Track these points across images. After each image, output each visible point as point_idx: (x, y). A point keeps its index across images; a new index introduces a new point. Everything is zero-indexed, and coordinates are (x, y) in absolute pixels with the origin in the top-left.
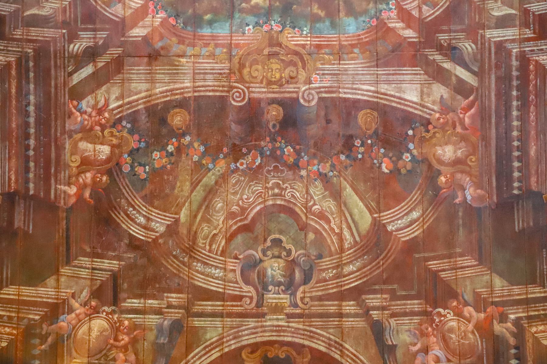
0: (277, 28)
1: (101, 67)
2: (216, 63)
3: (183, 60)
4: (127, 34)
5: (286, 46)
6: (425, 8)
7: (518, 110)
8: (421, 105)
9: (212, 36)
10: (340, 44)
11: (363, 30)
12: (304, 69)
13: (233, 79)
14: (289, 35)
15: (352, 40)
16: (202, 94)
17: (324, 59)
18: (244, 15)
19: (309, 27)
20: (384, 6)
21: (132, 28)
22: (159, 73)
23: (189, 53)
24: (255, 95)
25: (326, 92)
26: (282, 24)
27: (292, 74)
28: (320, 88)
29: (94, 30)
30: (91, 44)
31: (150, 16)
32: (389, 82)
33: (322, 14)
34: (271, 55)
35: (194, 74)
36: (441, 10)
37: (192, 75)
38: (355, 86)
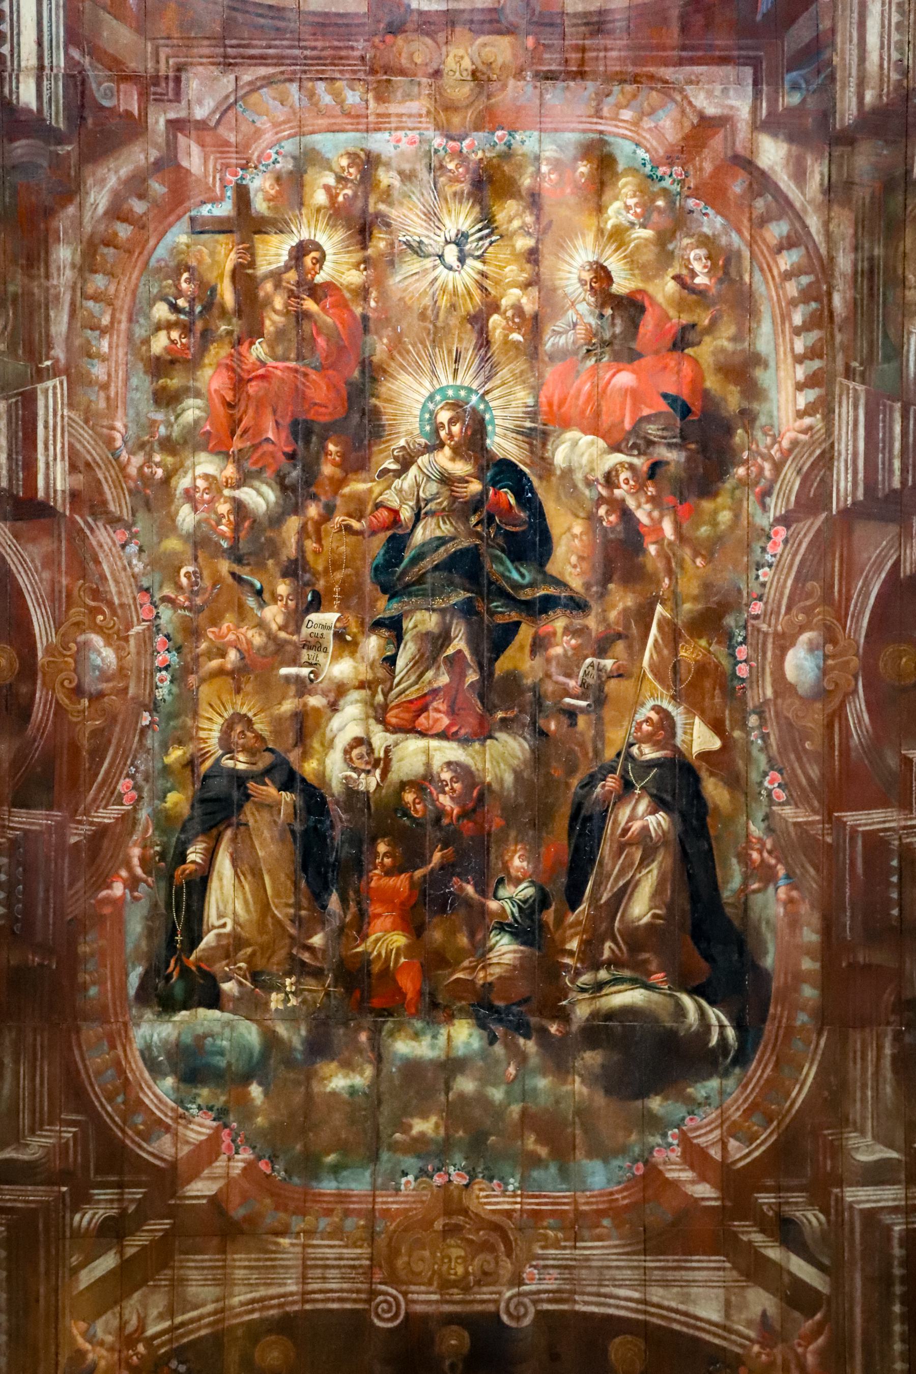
0: (459, 1180)
1: (134, 1256)
2: (346, 1247)
3: (285, 1241)
4: (179, 1193)
5: (476, 1215)
6: (733, 1143)
7: (903, 1341)
8: (724, 1328)
9: (339, 1195)
10: (576, 1210)
11: (619, 1183)
12: (509, 1256)
13: (378, 1276)
14: (482, 1194)
15: (597, 1203)
16: (320, 1306)
17: (546, 1237)
18: (399, 1156)
19: (518, 1177)
20: (658, 1140)
21: (189, 1182)
22: (240, 1267)
23: (295, 1229)
24: (419, 1308)
25: (549, 1301)
26: (468, 1173)
27: (487, 1268)
28: (539, 1292)
29: (120, 1185)
31: (224, 1157)
32: (666, 1284)
33: (543, 1151)
34: (451, 1231)
35: (305, 1267)
36: (763, 1148)
37: (300, 1269)
38: (603, 1290)
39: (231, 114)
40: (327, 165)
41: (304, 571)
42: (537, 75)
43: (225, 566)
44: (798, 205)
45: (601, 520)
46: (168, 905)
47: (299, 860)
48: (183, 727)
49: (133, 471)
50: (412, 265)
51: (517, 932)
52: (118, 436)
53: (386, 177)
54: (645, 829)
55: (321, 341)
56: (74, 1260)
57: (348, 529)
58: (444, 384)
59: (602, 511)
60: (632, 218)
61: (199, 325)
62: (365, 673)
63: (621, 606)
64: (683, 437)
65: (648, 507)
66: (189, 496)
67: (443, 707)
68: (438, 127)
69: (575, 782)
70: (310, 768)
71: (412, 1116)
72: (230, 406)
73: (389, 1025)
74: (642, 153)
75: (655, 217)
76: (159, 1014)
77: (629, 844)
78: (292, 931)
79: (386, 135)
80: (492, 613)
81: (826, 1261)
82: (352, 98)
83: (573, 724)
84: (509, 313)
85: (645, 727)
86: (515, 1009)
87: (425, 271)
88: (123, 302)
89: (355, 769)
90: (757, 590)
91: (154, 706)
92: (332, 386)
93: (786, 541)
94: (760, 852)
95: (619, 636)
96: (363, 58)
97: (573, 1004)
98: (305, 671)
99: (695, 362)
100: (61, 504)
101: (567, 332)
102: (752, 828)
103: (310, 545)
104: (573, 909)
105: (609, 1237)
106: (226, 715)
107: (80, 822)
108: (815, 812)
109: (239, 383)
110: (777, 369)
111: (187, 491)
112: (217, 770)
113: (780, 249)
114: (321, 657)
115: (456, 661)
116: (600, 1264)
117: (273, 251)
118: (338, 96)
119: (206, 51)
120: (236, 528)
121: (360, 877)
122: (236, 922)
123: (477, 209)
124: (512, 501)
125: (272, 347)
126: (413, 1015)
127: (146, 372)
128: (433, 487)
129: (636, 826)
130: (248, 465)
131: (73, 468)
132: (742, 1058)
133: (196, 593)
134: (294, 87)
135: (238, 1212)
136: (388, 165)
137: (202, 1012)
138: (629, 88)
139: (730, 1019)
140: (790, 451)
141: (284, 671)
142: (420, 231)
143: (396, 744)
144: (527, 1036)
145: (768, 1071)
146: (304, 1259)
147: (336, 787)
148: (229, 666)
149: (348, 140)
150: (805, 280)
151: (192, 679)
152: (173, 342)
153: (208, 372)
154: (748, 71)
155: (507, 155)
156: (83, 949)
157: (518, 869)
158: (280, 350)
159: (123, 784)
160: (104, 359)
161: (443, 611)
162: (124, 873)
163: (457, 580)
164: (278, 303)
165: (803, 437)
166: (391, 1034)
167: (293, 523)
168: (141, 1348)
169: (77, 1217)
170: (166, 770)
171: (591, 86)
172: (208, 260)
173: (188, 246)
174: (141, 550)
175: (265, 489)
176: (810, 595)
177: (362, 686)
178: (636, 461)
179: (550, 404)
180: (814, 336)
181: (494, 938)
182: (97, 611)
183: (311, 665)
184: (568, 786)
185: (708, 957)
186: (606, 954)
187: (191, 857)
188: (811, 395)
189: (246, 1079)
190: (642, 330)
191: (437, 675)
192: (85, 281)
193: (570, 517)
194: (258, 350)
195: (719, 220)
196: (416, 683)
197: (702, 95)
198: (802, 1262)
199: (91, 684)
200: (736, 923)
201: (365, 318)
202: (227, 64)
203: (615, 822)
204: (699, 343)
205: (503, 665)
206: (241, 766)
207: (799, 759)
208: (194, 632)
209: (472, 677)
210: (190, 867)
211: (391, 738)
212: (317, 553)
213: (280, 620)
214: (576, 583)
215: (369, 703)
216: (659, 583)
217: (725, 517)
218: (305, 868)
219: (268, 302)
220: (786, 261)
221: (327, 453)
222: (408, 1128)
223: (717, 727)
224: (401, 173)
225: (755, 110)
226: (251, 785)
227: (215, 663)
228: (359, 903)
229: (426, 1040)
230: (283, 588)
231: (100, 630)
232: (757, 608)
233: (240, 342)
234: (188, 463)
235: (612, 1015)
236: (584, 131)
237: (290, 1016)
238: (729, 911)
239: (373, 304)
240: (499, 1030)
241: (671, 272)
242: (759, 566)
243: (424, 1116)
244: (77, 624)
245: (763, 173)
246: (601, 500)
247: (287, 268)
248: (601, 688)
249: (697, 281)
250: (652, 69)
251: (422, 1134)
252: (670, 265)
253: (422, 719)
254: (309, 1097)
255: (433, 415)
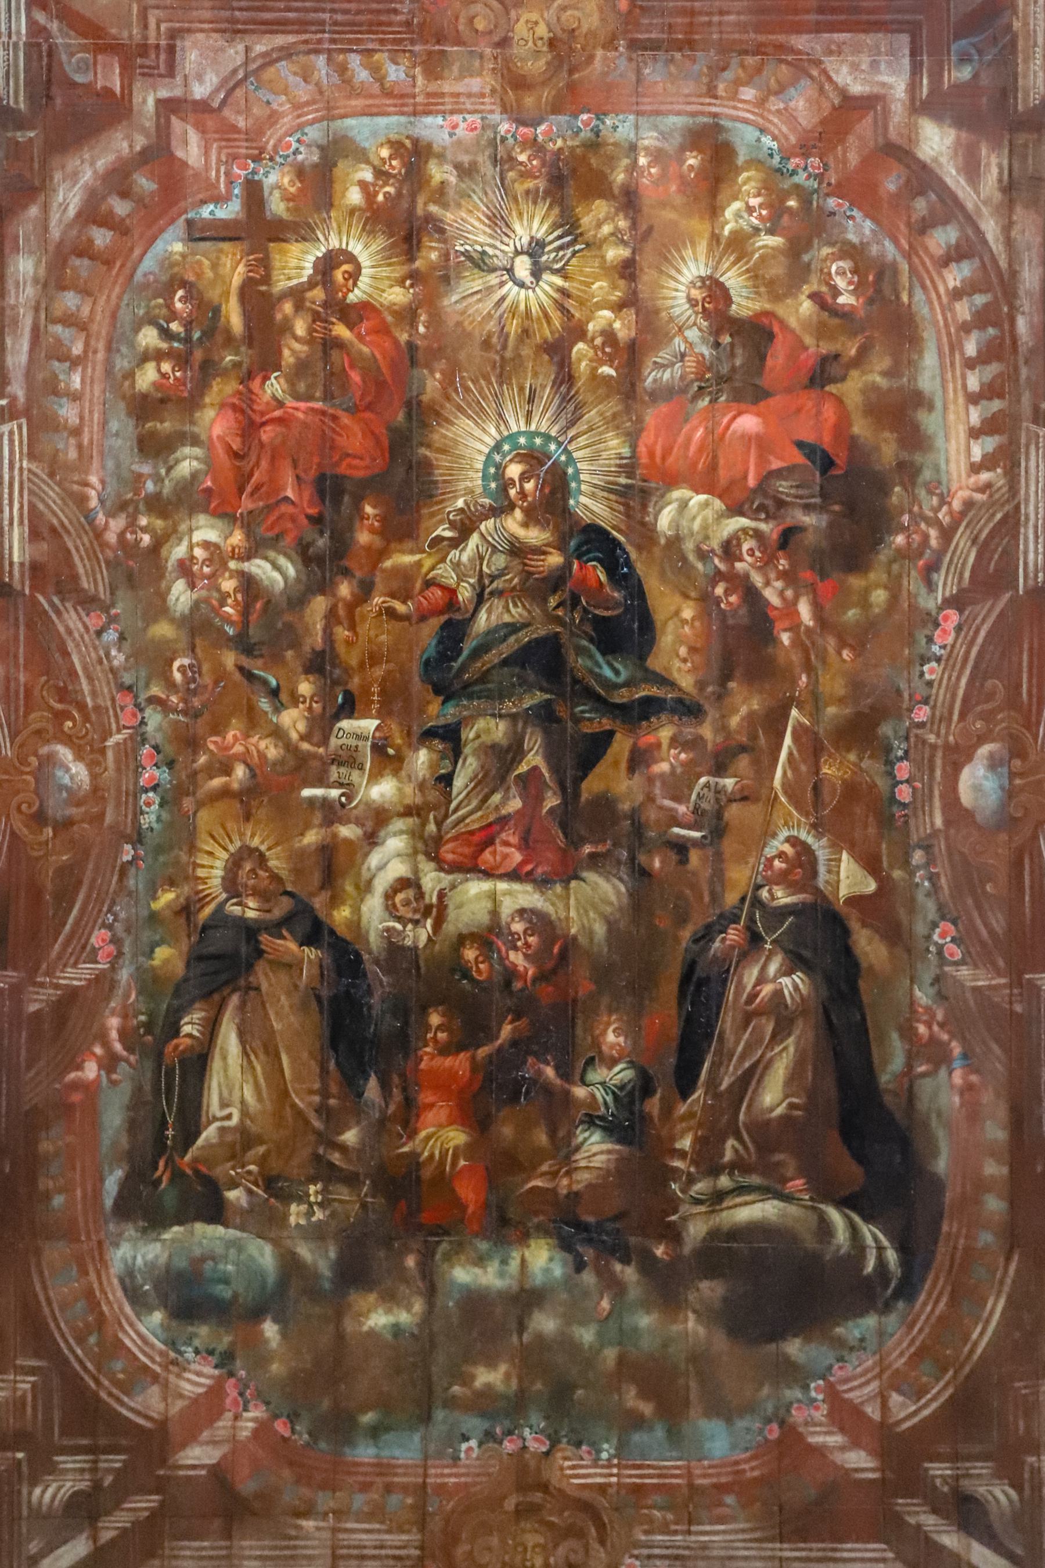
0: (536, 1445)
2: (389, 1531)
3: (309, 1524)
4: (171, 1462)
5: (560, 1490)
6: (895, 1398)
9: (378, 1465)
10: (691, 1486)
11: (747, 1449)
14: (567, 1463)
15: (719, 1475)
17: (651, 1520)
18: (457, 1414)
19: (615, 1441)
20: (798, 1394)
21: (183, 1445)
22: (250, 1558)
23: (321, 1507)
26: (549, 1437)
30: (84, 1485)
31: (229, 1415)
33: (647, 1408)
34: (522, 1512)
35: (335, 1557)
36: (934, 1405)
37: (329, 1561)
39: (239, 93)
40: (362, 156)
41: (334, 666)
42: (634, 45)
43: (230, 659)
44: (970, 206)
45: (718, 601)
46: (156, 1091)
47: (327, 1034)
48: (177, 863)
49: (111, 537)
50: (473, 283)
51: (611, 1129)
52: (93, 493)
53: (438, 172)
54: (778, 993)
55: (355, 377)
56: (34, 1547)
57: (391, 613)
58: (514, 429)
59: (719, 590)
60: (756, 222)
61: (198, 355)
62: (411, 795)
63: (744, 710)
64: (823, 494)
65: (779, 584)
66: (185, 568)
67: (514, 840)
68: (504, 110)
69: (686, 934)
70: (342, 914)
71: (475, 1363)
72: (236, 455)
73: (444, 1247)
74: (767, 141)
75: (785, 220)
76: (144, 1231)
77: (758, 1013)
78: (317, 1124)
79: (439, 120)
80: (577, 720)
81: (1019, 1551)
82: (395, 73)
83: (684, 861)
84: (598, 341)
85: (777, 863)
86: (610, 1226)
87: (489, 290)
88: (100, 326)
89: (399, 919)
90: (921, 691)
91: (138, 838)
92: (370, 432)
93: (959, 629)
94: (929, 1027)
95: (743, 749)
96: (408, 24)
97: (684, 1219)
98: (334, 793)
99: (839, 401)
100: (17, 579)
101: (673, 364)
102: (918, 993)
103: (342, 633)
104: (685, 1095)
105: (733, 1519)
106: (232, 849)
107: (42, 985)
108: (999, 974)
109: (249, 428)
110: (945, 408)
111: (181, 563)
112: (219, 919)
113: (946, 261)
114: (355, 777)
115: (530, 782)
116: (722, 1553)
117: (293, 263)
118: (376, 71)
119: (207, 15)
120: (246, 611)
121: (406, 1056)
122: (245, 1113)
123: (556, 211)
124: (603, 577)
125: (292, 383)
126: (476, 1235)
127: (129, 414)
128: (501, 561)
129: (767, 989)
130: (261, 531)
131: (35, 535)
132: (907, 1289)
133: (195, 693)
134: (321, 60)
135: (247, 1486)
136: (441, 157)
137: (199, 1227)
138: (751, 60)
139: (891, 1240)
140: (963, 514)
141: (307, 792)
142: (481, 239)
143: (453, 887)
144: (626, 1261)
145: (942, 1305)
146: (334, 1548)
147: (374, 940)
148: (235, 786)
149: (391, 124)
150: (980, 300)
151: (188, 803)
152: (164, 376)
153: (210, 414)
154: (904, 40)
155: (595, 144)
156: (45, 1146)
157: (612, 1047)
158: (302, 387)
159: (98, 937)
160: (75, 397)
161: (513, 717)
162: (98, 1050)
163: (532, 677)
164: (300, 328)
165: (978, 497)
166: (447, 1257)
167: (319, 604)
169: (37, 1491)
170: (154, 918)
171: (703, 59)
172: (209, 274)
173: (184, 256)
174: (122, 638)
175: (282, 561)
176: (990, 696)
177: (408, 812)
178: (763, 527)
179: (651, 454)
180: (993, 369)
181: (581, 1135)
182: (61, 716)
183: (341, 785)
184: (677, 940)
185: (861, 1159)
186: (728, 1156)
187: (187, 1029)
188: (991, 443)
189: (257, 1314)
190: (769, 362)
191: (506, 799)
192: (51, 299)
193: (678, 599)
194: (275, 386)
195: (868, 225)
196: (478, 808)
197: (845, 69)
198: (987, 1552)
199: (57, 807)
200: (898, 1116)
201: (411, 346)
202: (233, 30)
203: (740, 986)
204: (843, 379)
205: (591, 786)
206: (251, 914)
207: (979, 907)
208: (192, 744)
209: (552, 801)
210: (184, 1043)
211: (447, 879)
212: (349, 643)
213: (302, 727)
214: (686, 682)
215: (416, 835)
216: (794, 682)
217: (879, 597)
218: (334, 1044)
219: (287, 327)
220: (955, 276)
221: (363, 517)
222: (467, 1380)
223: (871, 864)
224: (458, 166)
225: (913, 87)
226: (264, 938)
227: (217, 782)
228: (404, 1089)
229: (493, 1267)
230: (305, 688)
231: (68, 740)
232: (922, 714)
233: (250, 376)
234: (183, 527)
235: (737, 1233)
236: (693, 114)
237: (316, 1234)
238: (888, 1099)
239: (422, 329)
240: (588, 1254)
241: (806, 289)
242: (924, 660)
243: (491, 1364)
244: (38, 732)
245: (924, 166)
246: (718, 576)
247: (311, 284)
248: (719, 815)
249: (841, 300)
250: (781, 38)
251: (488, 1386)
252: (805, 281)
253: (487, 855)
254: (340, 1336)
255: (500, 468)
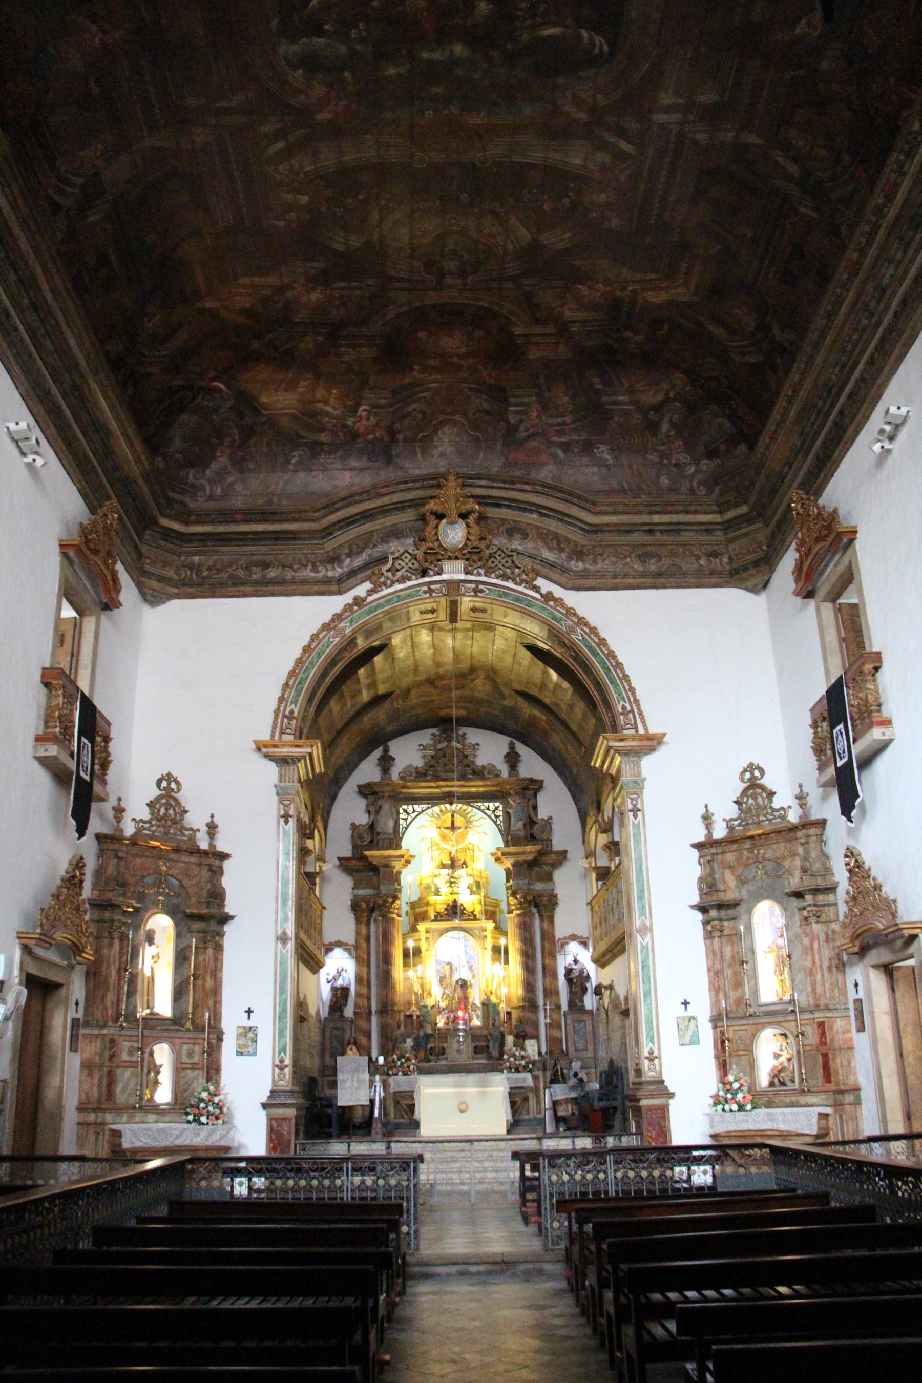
0: (455, 110)
3: (368, 137)
168: (302, 175)
